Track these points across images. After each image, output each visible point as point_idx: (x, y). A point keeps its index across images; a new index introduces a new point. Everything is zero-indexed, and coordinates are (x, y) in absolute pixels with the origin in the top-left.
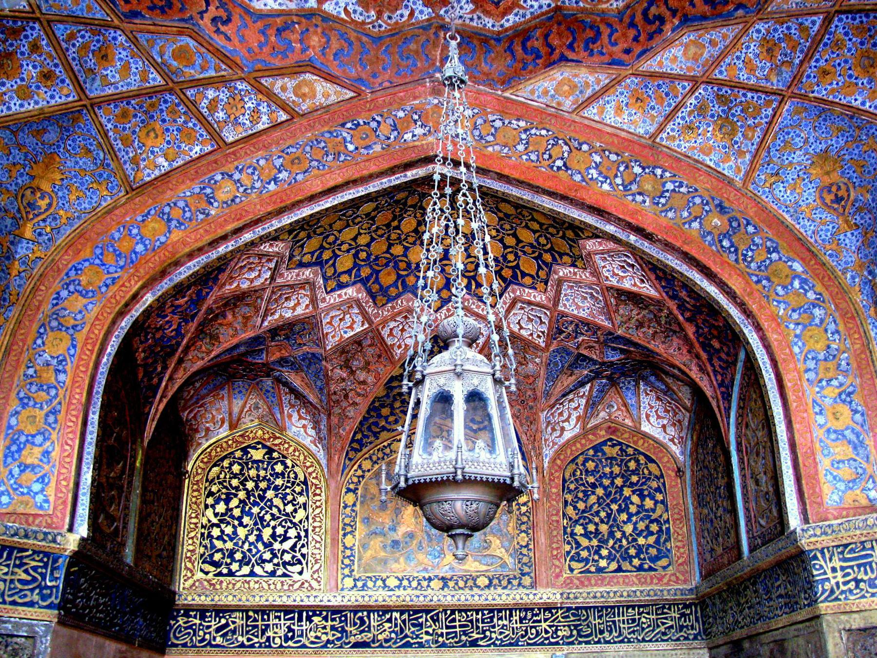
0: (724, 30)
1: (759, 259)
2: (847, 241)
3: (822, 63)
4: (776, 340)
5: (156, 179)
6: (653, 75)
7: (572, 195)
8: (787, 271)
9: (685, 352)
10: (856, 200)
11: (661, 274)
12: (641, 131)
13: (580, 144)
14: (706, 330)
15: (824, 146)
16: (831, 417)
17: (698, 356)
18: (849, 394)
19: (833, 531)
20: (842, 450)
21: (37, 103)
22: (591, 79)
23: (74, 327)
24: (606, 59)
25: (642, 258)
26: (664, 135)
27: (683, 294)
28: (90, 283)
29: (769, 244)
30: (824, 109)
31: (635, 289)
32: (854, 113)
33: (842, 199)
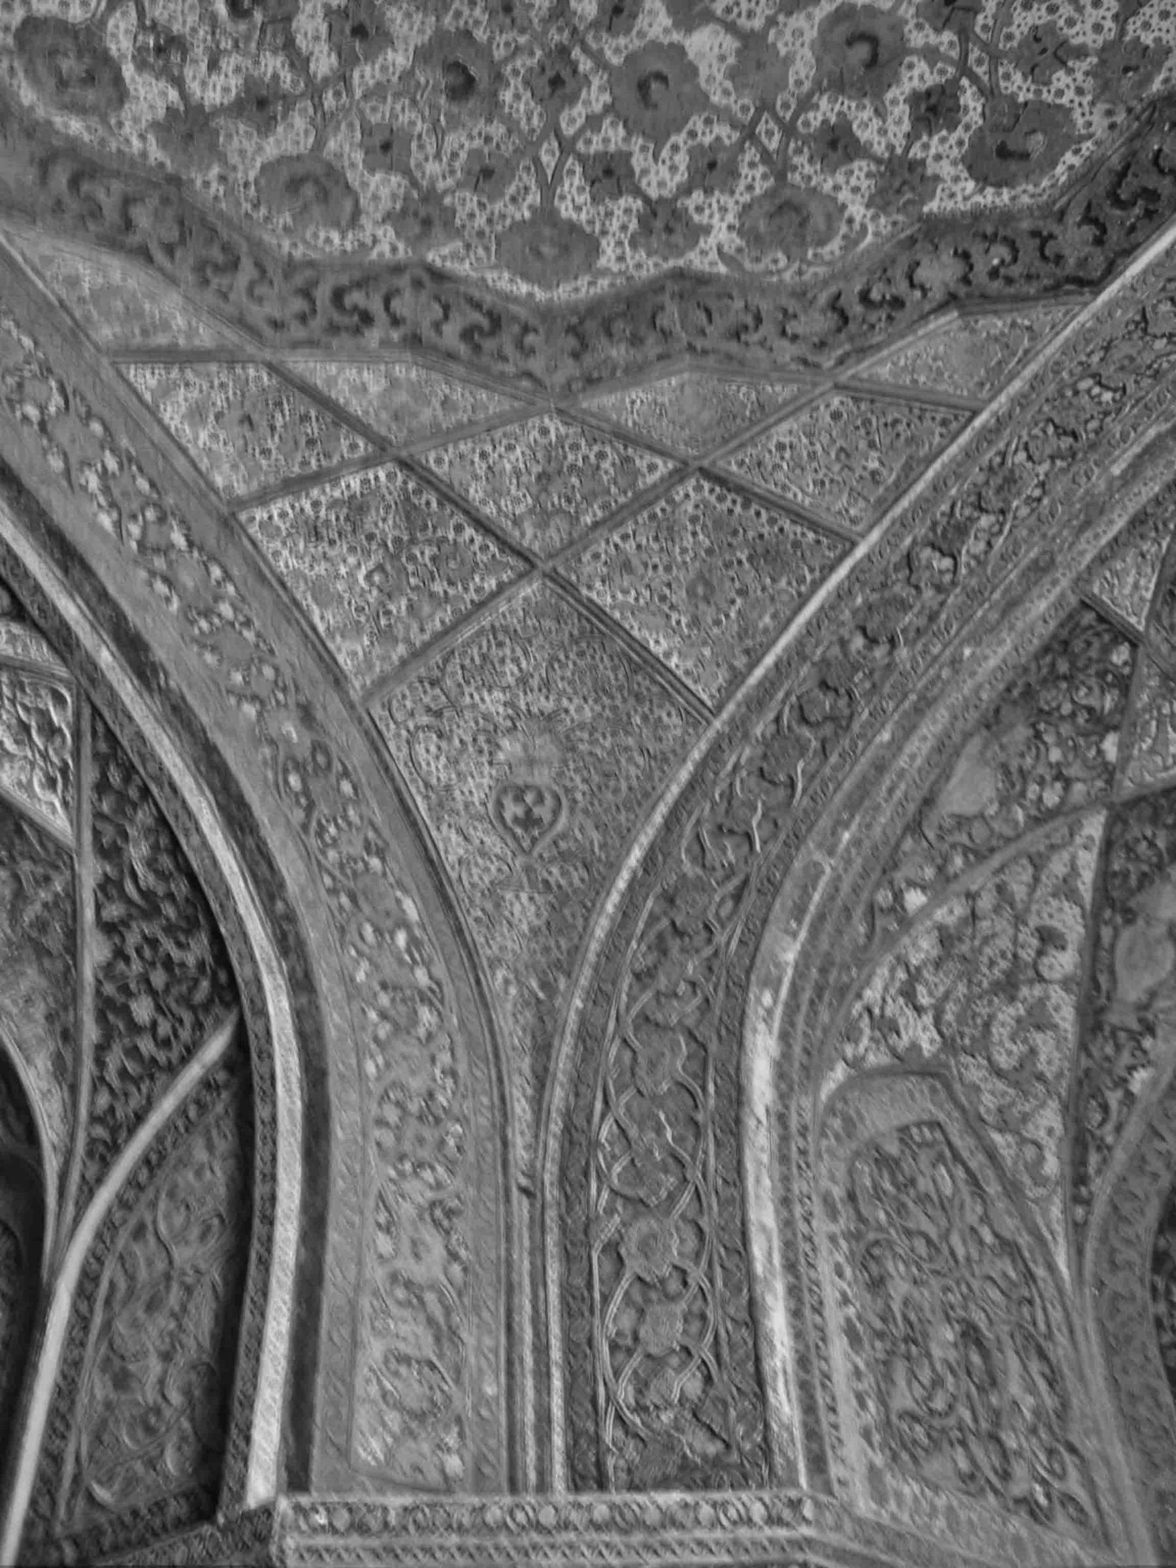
0: (483, 395)
1: (346, 849)
2: (517, 909)
3: (630, 547)
4: (336, 1026)
6: (308, 391)
7: (30, 481)
8: (390, 904)
9: (39, 1011)
10: (564, 836)
11: (115, 777)
12: (219, 481)
13: (89, 415)
14: (137, 967)
15: (549, 706)
16: (406, 1247)
17: (68, 1036)
18: (450, 1213)
19: (386, 1524)
20: (412, 1334)
22: (180, 321)
24: (229, 309)
25: (96, 712)
26: (260, 514)
27: (137, 852)
29: (371, 835)
30: (598, 624)
31: (20, 798)
32: (643, 662)
33: (538, 822)
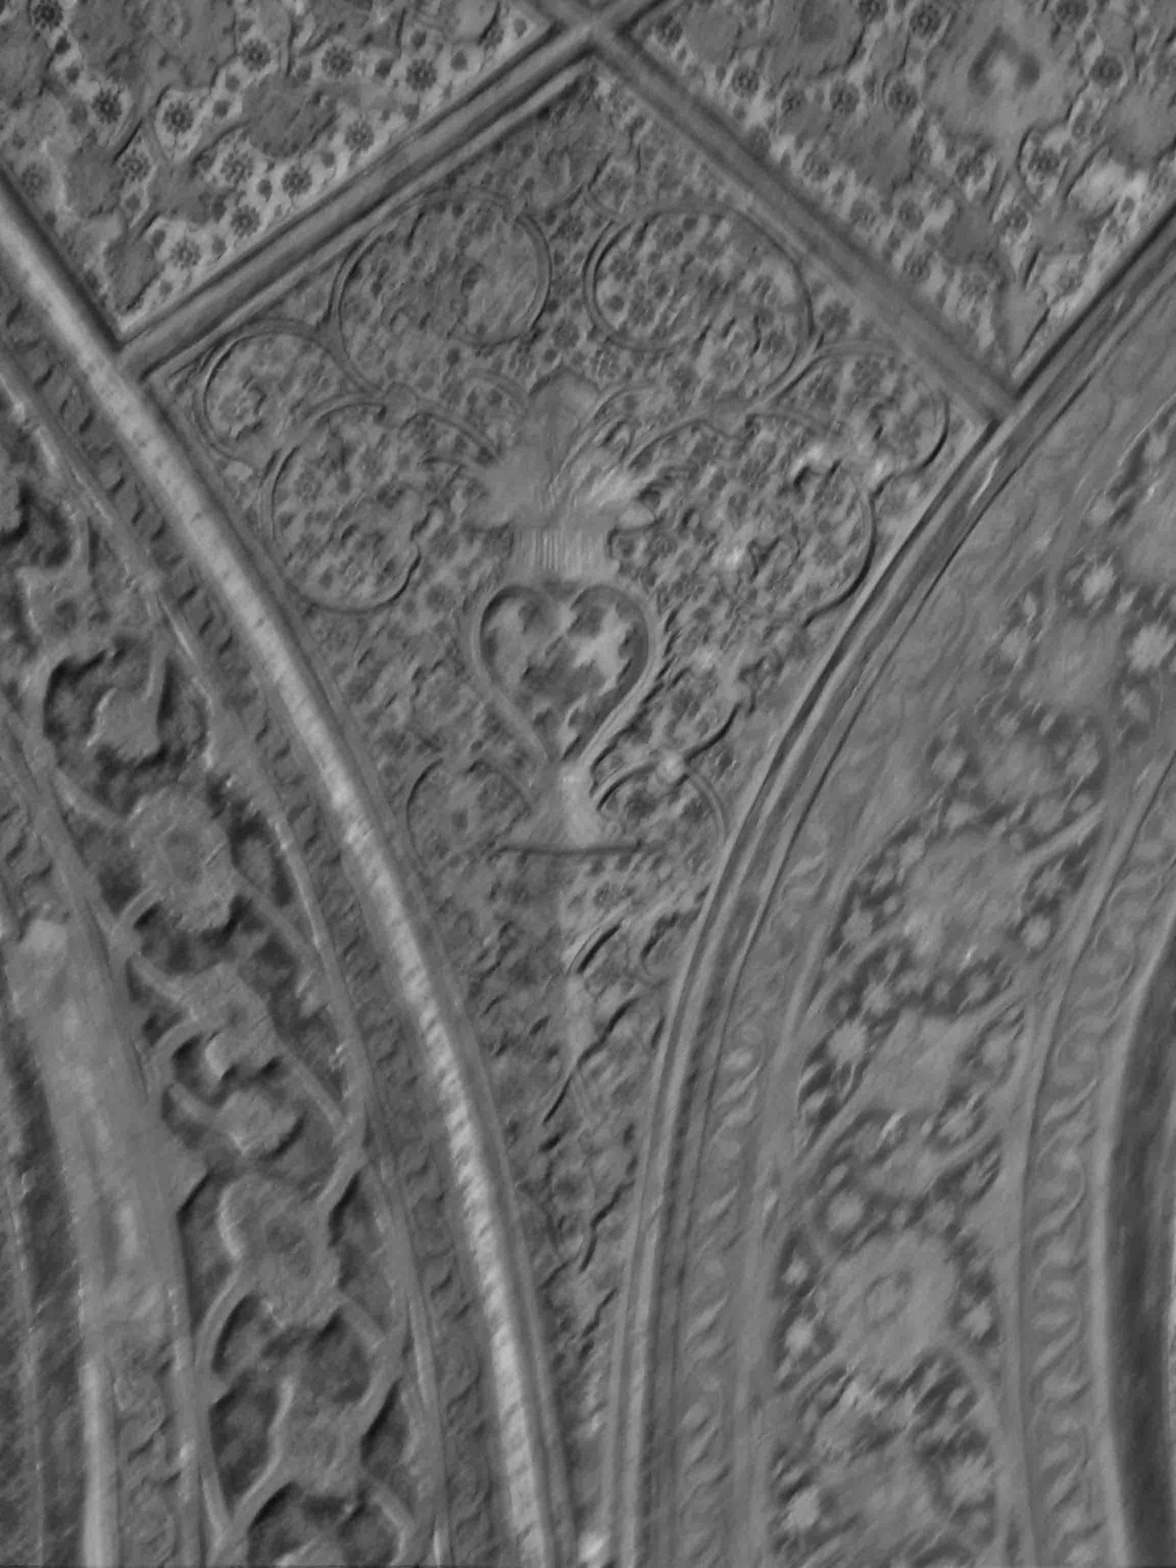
5: (1112, 284)
21: (359, 138)
23: (949, 1183)
28: (955, 933)
